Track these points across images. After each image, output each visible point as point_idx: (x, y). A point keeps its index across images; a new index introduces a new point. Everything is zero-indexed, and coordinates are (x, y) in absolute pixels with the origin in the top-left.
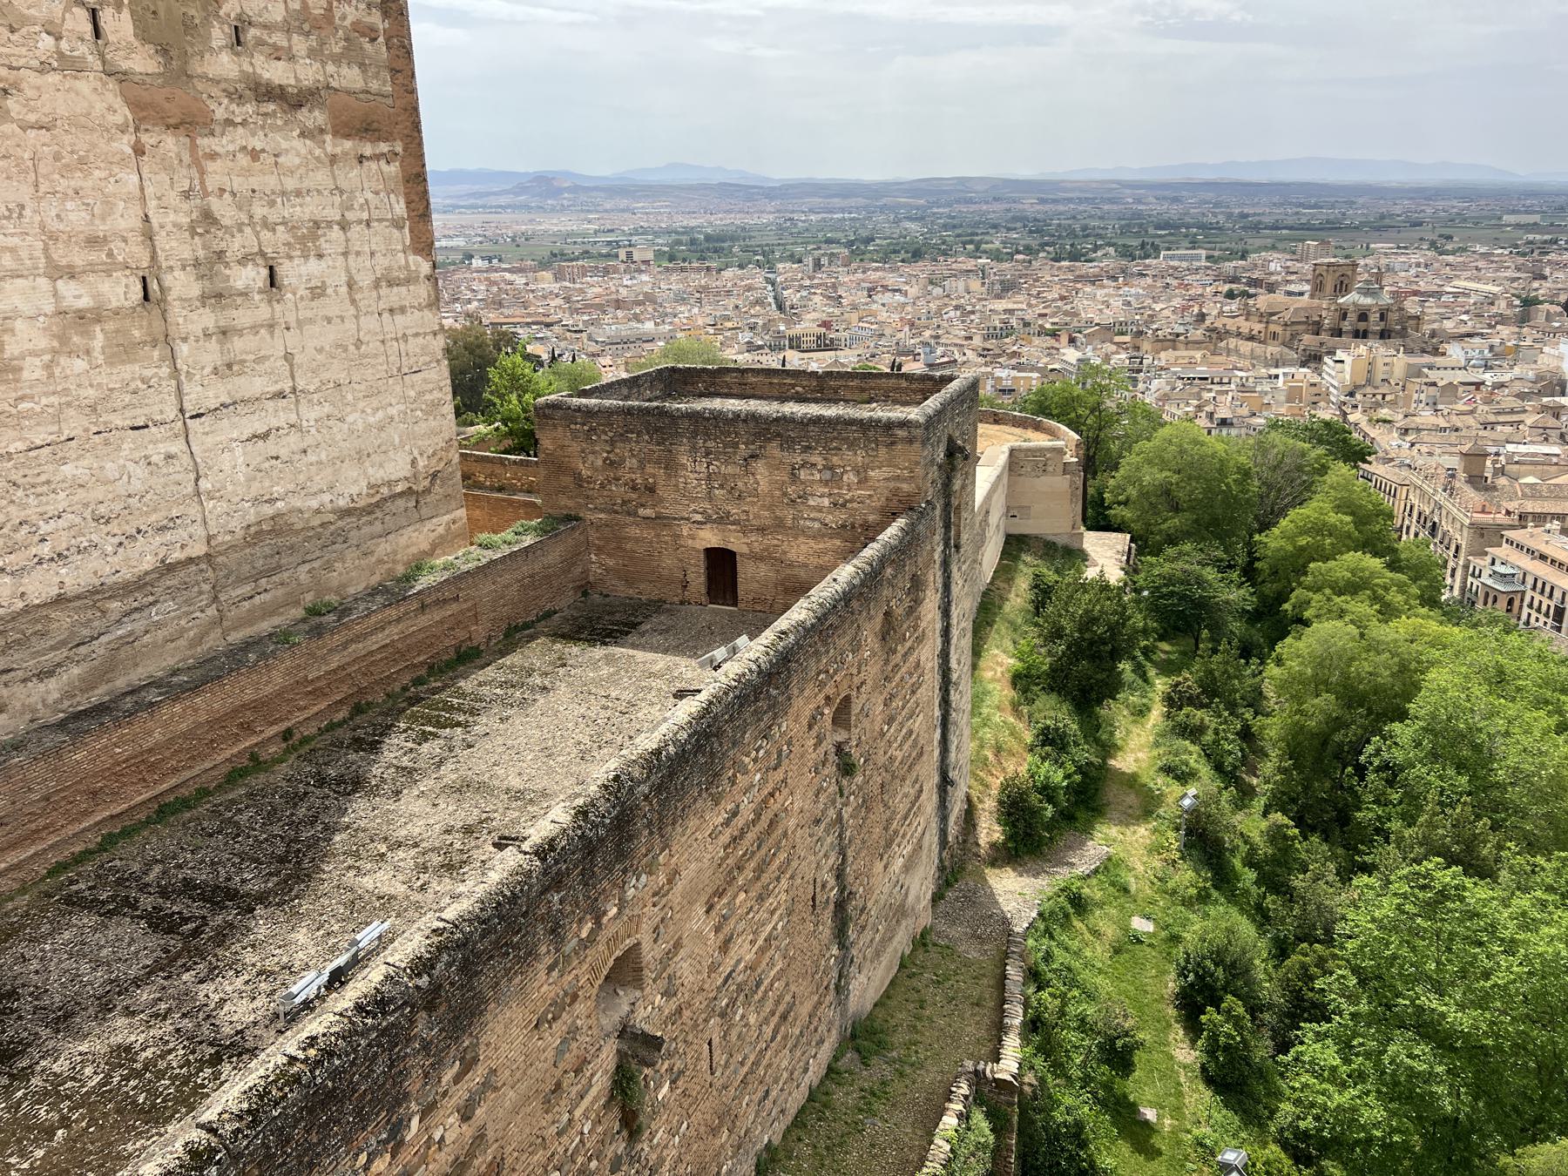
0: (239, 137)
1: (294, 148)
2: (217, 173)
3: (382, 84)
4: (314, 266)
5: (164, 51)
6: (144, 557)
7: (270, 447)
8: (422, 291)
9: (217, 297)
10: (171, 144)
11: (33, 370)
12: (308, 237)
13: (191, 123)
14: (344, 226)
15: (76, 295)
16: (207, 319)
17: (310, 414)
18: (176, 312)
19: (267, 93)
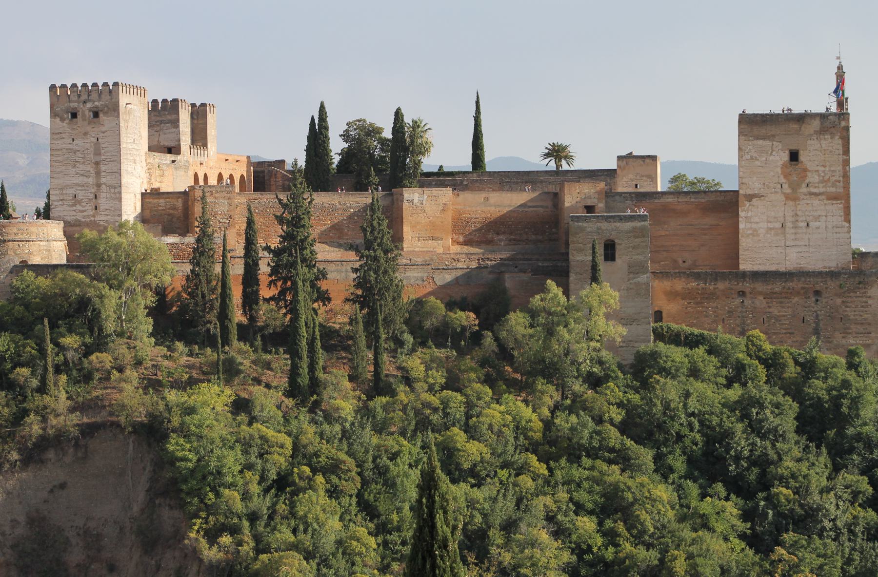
0: (805, 201)
1: (816, 202)
2: (799, 207)
3: (841, 190)
4: (817, 224)
5: (793, 189)
6: (773, 268)
7: (802, 254)
8: (846, 230)
9: (796, 227)
10: (791, 203)
11: (762, 235)
12: (817, 218)
13: (795, 199)
14: (826, 216)
15: (770, 225)
16: (793, 231)
17: (811, 250)
18: (787, 229)
19: (811, 194)
